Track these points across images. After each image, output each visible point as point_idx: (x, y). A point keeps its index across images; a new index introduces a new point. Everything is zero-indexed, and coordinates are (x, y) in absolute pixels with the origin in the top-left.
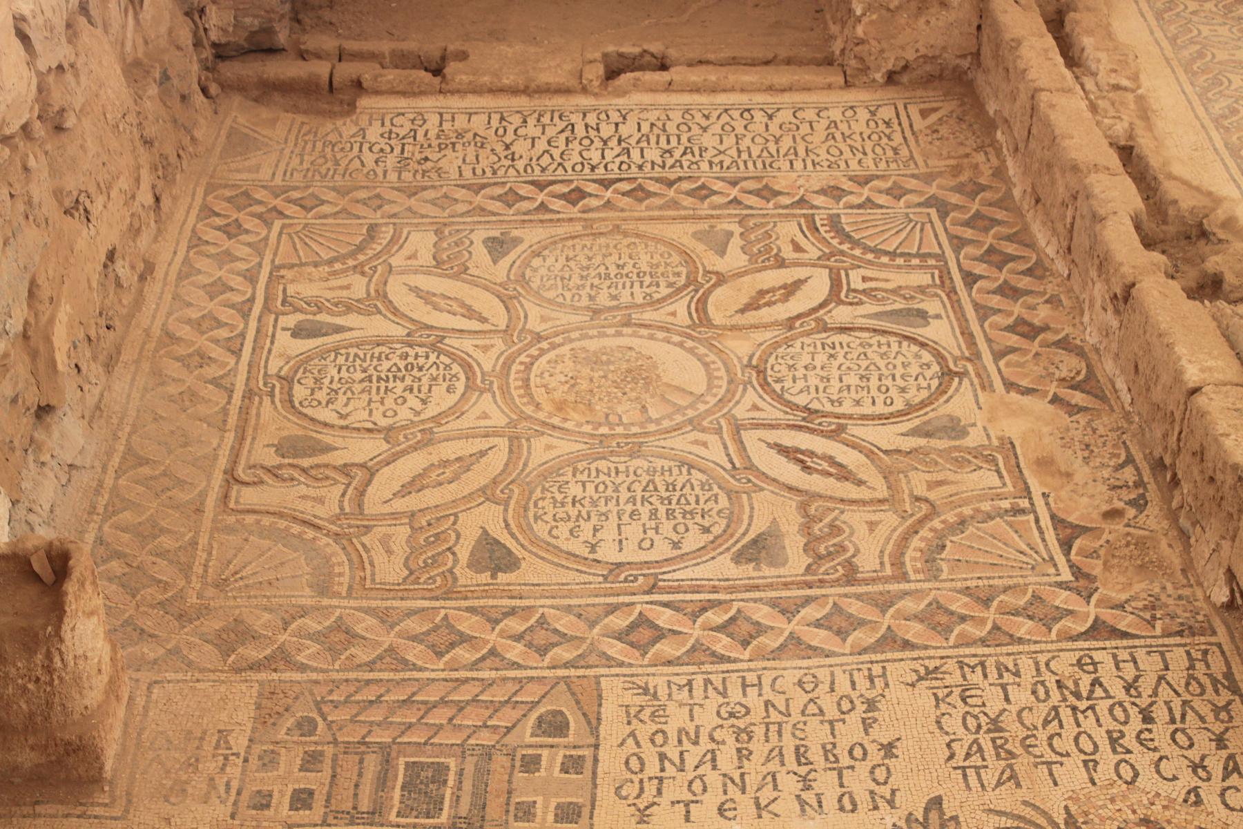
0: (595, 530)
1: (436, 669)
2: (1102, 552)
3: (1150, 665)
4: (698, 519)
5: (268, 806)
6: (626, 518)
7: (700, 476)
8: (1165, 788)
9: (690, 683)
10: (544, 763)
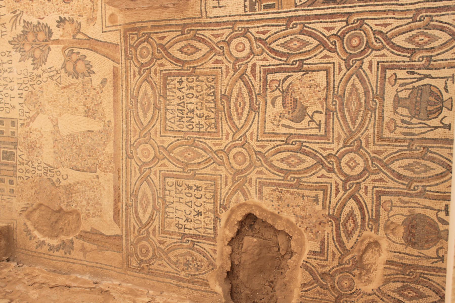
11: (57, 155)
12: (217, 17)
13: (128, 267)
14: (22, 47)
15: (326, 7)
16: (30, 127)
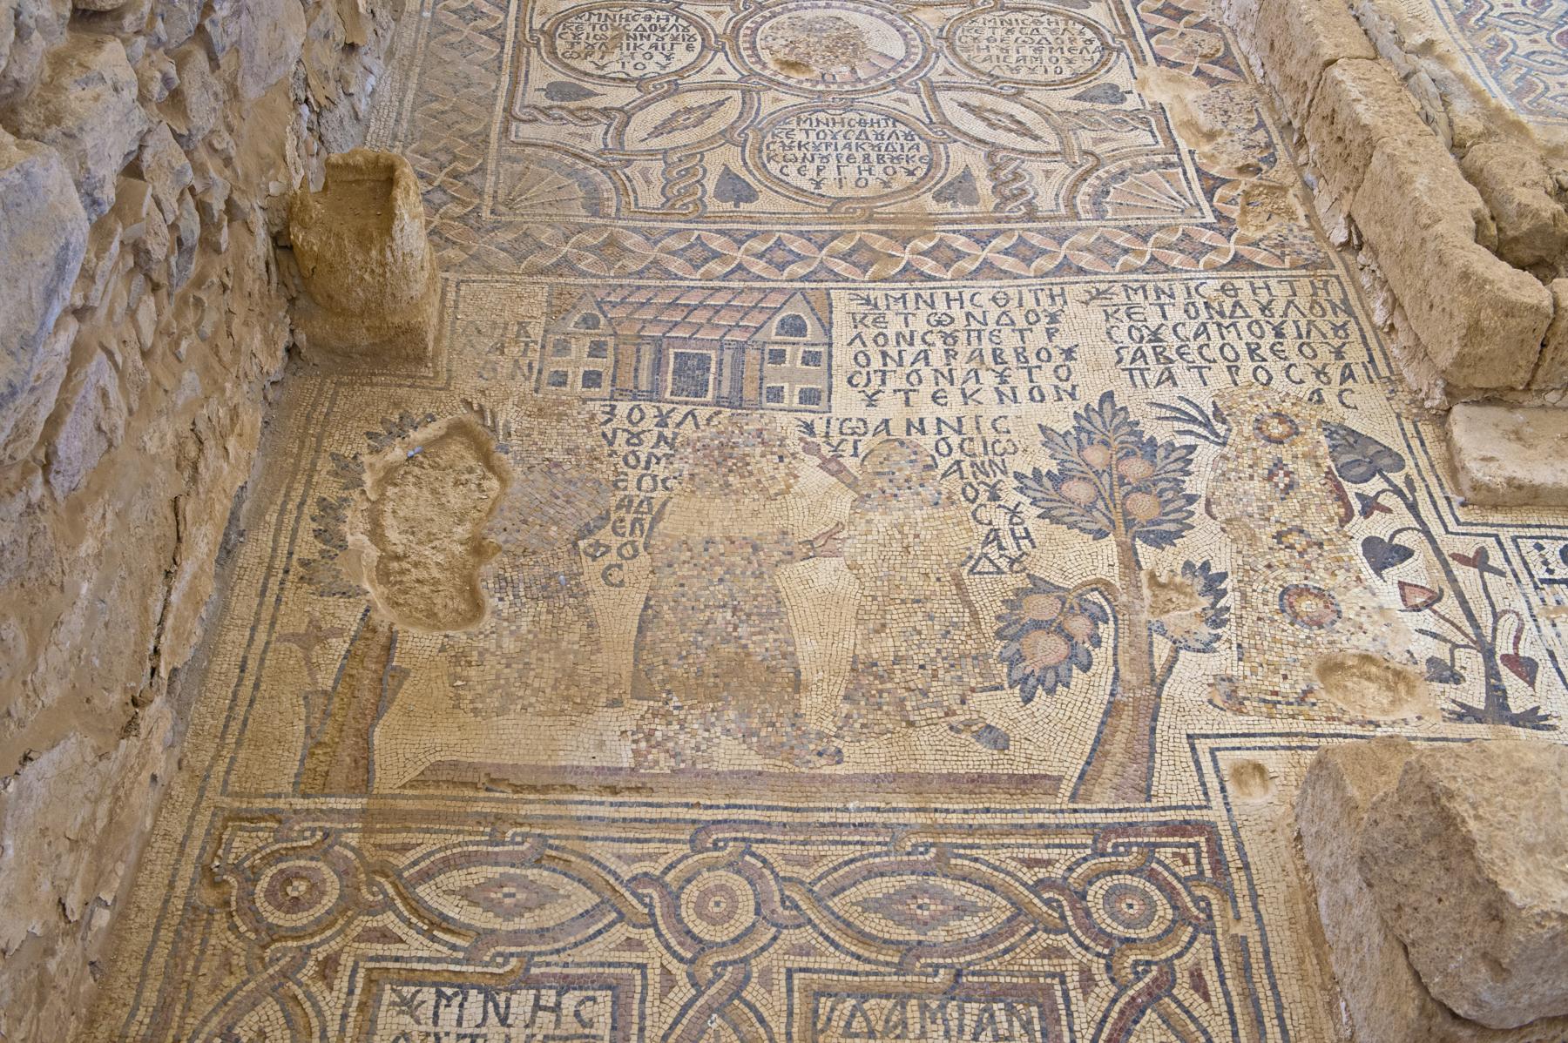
0: (819, 170)
1: (695, 279)
2: (1239, 200)
3: (1281, 292)
4: (904, 163)
5: (565, 383)
6: (844, 161)
7: (903, 128)
8: (1293, 389)
9: (904, 296)
10: (788, 356)
11: (700, 548)
13: (227, 820)
14: (1098, 437)
16: (802, 455)
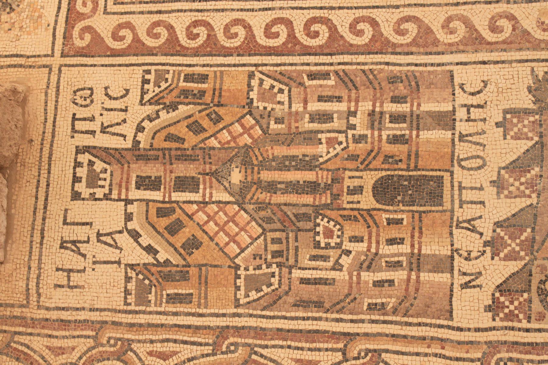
12: (63, 309)
15: (301, 314)
